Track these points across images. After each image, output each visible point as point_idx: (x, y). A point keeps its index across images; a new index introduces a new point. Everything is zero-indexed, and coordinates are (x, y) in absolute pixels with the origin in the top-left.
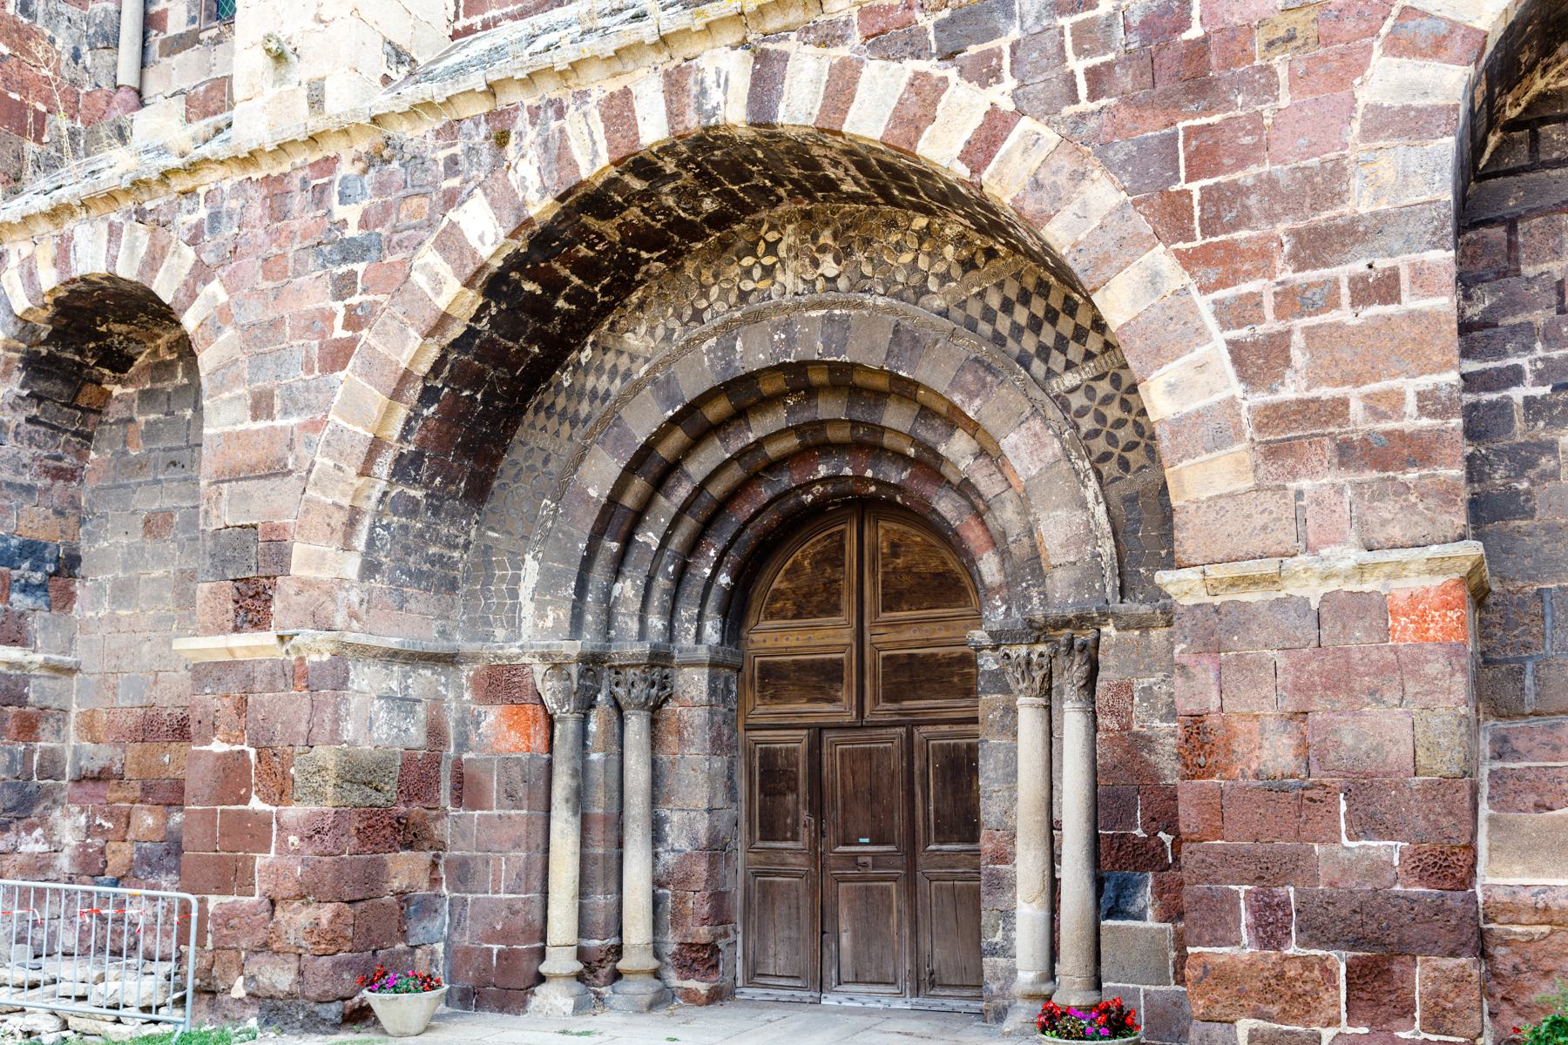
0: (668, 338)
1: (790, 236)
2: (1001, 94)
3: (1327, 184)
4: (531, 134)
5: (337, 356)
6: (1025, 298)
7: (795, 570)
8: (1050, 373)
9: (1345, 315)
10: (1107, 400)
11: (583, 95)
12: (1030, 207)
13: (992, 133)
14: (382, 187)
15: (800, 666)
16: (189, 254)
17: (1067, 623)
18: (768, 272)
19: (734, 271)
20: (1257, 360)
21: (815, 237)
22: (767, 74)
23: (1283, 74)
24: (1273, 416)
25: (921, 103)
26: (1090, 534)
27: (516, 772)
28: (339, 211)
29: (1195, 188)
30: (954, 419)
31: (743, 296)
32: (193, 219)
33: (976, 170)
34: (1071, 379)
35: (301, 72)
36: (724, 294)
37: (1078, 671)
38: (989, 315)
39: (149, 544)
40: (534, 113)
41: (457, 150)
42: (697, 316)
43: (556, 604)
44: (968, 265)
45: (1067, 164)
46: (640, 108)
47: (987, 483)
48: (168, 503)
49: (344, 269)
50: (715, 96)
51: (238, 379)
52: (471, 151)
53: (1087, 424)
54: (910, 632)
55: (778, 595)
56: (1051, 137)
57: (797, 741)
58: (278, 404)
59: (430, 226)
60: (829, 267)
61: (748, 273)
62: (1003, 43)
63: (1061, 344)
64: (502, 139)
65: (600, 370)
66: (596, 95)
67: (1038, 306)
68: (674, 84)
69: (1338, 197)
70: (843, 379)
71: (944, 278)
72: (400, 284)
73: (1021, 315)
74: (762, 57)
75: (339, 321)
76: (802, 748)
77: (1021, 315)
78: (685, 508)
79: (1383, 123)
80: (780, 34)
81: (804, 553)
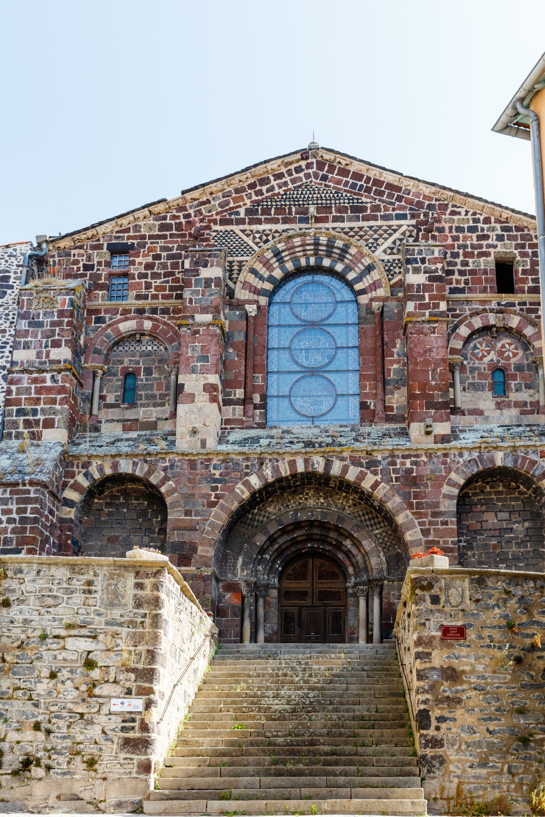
0: (280, 509)
1: (311, 493)
2: (379, 478)
3: (437, 505)
4: (269, 464)
5: (213, 505)
6: (367, 514)
7: (294, 569)
9: (439, 527)
11: (284, 459)
12: (384, 499)
13: (375, 485)
14: (226, 468)
15: (296, 592)
16: (163, 474)
17: (377, 580)
18: (306, 499)
19: (297, 498)
20: (425, 532)
22: (328, 464)
24: (427, 542)
25: (362, 477)
26: (381, 563)
27: (236, 609)
28: (213, 471)
30: (350, 536)
31: (300, 503)
32: (164, 465)
33: (373, 490)
34: (377, 531)
35: (199, 436)
36: (294, 502)
37: (378, 590)
38: (359, 516)
39: (109, 544)
40: (270, 460)
41: (249, 464)
42: (288, 506)
43: (247, 569)
44: (355, 505)
46: (298, 464)
47: (354, 551)
48: (117, 534)
50: (316, 466)
51: (180, 506)
52: (252, 465)
53: (381, 541)
54: (327, 585)
55: (289, 574)
56: (388, 487)
57: (296, 610)
58: (193, 514)
60: (322, 500)
61: (301, 498)
62: (379, 469)
63: (375, 524)
64: (262, 464)
65: (260, 515)
66: (287, 460)
67: (370, 516)
68: (306, 461)
69: (439, 507)
70: (322, 525)
72: (232, 490)
73: (367, 517)
74: (327, 460)
75: (213, 497)
76: (296, 612)
77: (367, 517)
78: (276, 550)
79: (446, 496)
80: (331, 457)
81: (297, 565)
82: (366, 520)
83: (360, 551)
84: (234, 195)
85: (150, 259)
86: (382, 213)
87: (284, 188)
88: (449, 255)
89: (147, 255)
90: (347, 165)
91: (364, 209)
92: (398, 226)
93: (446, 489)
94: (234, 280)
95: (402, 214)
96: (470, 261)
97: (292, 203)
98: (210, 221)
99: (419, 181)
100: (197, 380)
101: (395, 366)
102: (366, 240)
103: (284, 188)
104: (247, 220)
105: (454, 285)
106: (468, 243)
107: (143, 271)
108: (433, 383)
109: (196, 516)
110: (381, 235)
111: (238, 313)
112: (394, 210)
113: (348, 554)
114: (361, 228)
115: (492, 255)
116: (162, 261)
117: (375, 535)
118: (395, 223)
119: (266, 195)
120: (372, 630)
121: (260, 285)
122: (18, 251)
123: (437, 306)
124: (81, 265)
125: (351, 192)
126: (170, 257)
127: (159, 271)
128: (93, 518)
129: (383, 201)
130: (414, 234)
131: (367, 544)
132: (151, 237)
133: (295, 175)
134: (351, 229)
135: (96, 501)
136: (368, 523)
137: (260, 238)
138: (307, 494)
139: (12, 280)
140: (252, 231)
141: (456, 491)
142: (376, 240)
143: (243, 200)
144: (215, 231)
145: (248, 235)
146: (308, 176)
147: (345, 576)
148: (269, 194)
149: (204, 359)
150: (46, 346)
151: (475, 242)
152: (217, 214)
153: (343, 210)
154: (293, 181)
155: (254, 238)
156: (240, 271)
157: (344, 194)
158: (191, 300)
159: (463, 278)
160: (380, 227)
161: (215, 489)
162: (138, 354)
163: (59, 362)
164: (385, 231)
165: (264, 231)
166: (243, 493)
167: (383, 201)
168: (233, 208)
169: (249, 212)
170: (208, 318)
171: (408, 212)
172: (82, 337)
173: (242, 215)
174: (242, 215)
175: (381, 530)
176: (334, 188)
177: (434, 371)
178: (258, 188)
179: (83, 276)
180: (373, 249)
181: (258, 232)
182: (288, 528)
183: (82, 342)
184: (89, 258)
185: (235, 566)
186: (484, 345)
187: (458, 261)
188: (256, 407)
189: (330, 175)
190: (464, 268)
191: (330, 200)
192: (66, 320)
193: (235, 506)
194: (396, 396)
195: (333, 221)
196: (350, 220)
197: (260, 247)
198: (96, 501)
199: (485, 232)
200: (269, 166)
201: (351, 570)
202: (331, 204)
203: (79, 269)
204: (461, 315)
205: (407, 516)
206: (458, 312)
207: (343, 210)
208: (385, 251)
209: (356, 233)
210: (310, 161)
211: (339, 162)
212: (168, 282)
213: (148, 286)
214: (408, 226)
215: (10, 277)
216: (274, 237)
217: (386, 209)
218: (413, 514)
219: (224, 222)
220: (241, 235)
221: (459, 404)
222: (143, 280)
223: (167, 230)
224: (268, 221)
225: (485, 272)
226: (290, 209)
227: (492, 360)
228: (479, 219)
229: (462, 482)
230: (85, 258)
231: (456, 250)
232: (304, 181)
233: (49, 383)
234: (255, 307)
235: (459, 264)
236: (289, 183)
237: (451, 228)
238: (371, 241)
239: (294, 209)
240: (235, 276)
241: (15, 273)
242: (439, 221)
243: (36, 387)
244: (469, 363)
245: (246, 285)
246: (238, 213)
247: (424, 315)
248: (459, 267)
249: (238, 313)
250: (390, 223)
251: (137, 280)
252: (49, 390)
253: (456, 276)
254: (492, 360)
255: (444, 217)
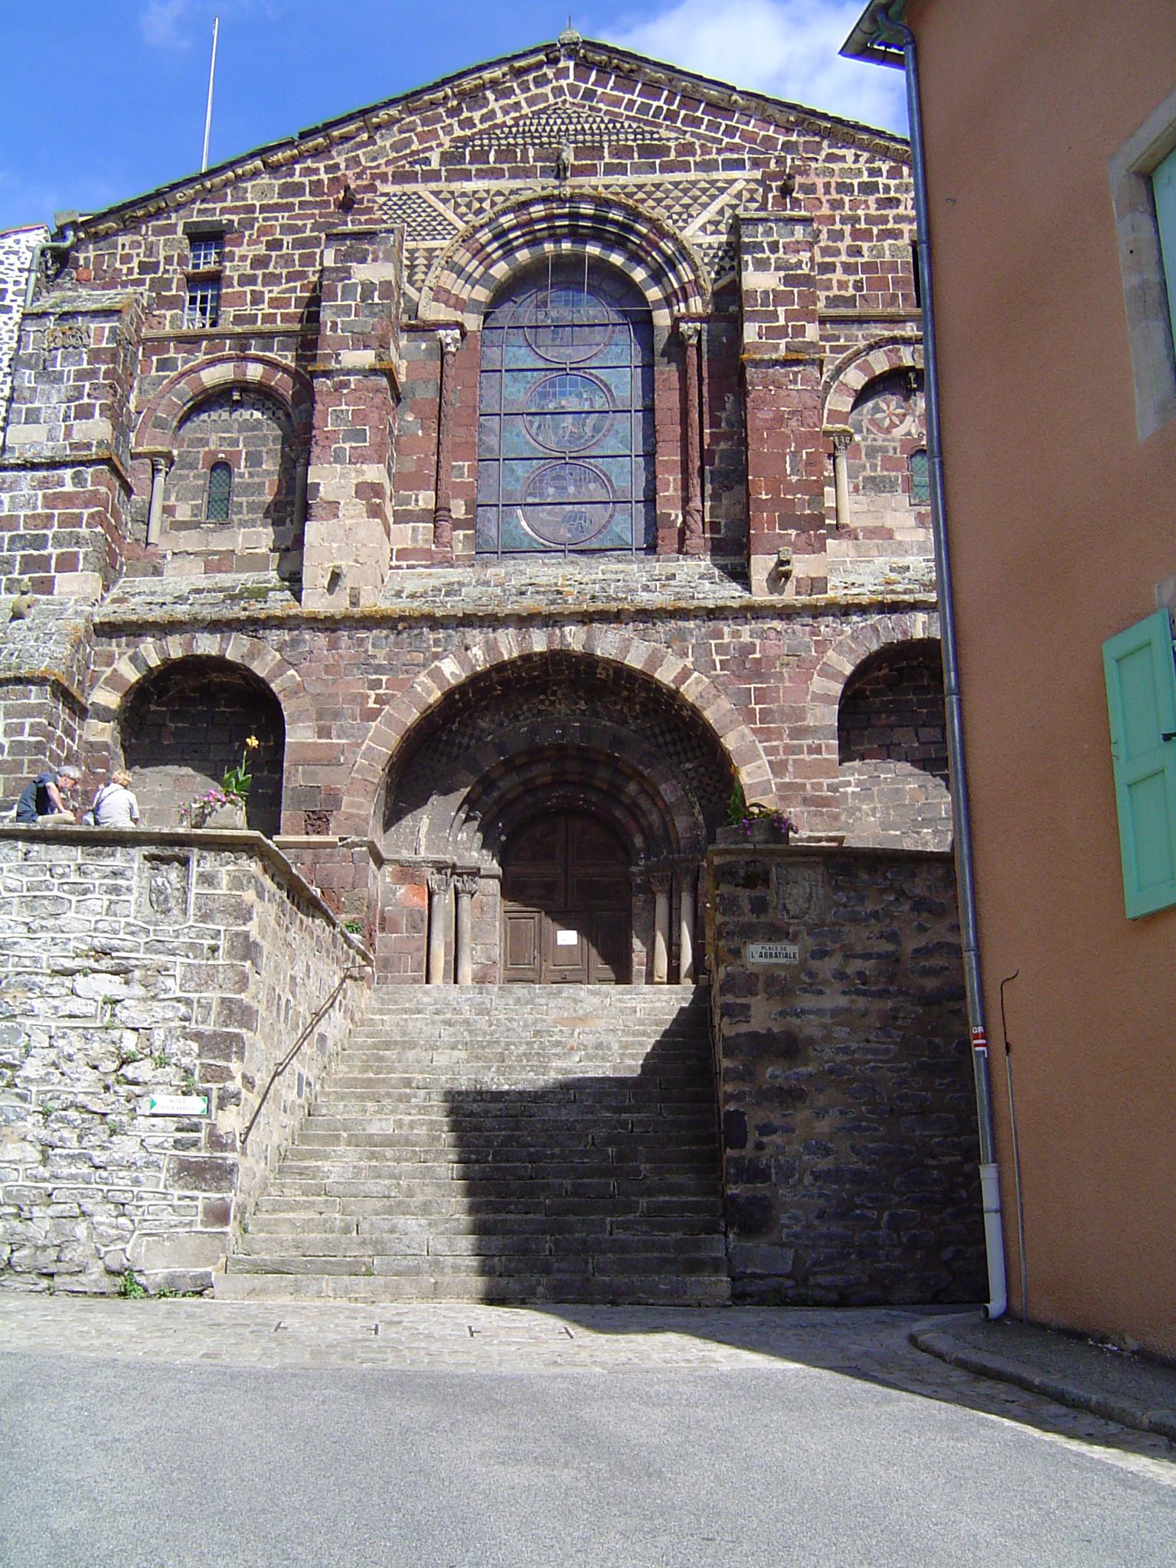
3: (800, 715)
5: (372, 715)
8: (680, 762)
9: (807, 758)
10: (703, 775)
12: (697, 704)
13: (685, 674)
18: (553, 703)
20: (778, 768)
21: (576, 692)
23: (786, 675)
29: (757, 707)
31: (540, 712)
34: (688, 766)
36: (529, 709)
38: (654, 735)
42: (516, 717)
44: (646, 714)
45: (714, 692)
47: (644, 803)
49: (374, 677)
53: (695, 784)
59: (424, 666)
61: (542, 702)
63: (685, 752)
65: (463, 736)
69: (804, 719)
71: (635, 718)
72: (407, 687)
73: (668, 738)
77: (668, 738)
79: (816, 697)
82: (666, 744)
83: (656, 805)
84: (419, 129)
85: (261, 249)
86: (698, 159)
87: (514, 114)
88: (824, 236)
89: (257, 242)
90: (631, 71)
91: (665, 151)
92: (726, 181)
93: (817, 684)
94: (419, 284)
95: (736, 160)
96: (865, 246)
97: (529, 140)
98: (374, 177)
99: (767, 100)
100: (343, 476)
101: (723, 446)
102: (668, 208)
103: (514, 114)
104: (443, 174)
105: (835, 292)
106: (860, 212)
107: (249, 272)
108: (794, 479)
109: (339, 737)
110: (695, 199)
111: (424, 346)
112: (719, 151)
113: (633, 810)
114: (657, 186)
115: (906, 235)
116: (285, 251)
117: (685, 772)
118: (721, 175)
119: (479, 127)
120: (679, 959)
121: (465, 292)
122: (23, 244)
123: (800, 331)
124: (135, 264)
125: (639, 120)
126: (298, 244)
127: (278, 271)
128: (147, 741)
129: (699, 136)
130: (758, 196)
131: (669, 792)
132: (264, 209)
133: (534, 91)
134: (640, 187)
135: (153, 708)
136: (672, 749)
137: (469, 206)
138: (554, 693)
139: (9, 296)
140: (452, 193)
141: (837, 688)
142: (687, 206)
143: (437, 137)
144: (382, 195)
145: (445, 201)
146: (558, 92)
147: (629, 855)
148: (486, 125)
149: (357, 435)
150: (66, 418)
151: (873, 212)
152: (387, 164)
153: (627, 152)
154: (531, 102)
155: (457, 205)
156: (428, 267)
157: (626, 125)
158: (334, 324)
159: (852, 278)
160: (694, 183)
161: (376, 685)
162: (236, 426)
163: (88, 446)
164: (704, 191)
165: (475, 192)
166: (429, 693)
167: (699, 136)
168: (418, 152)
169: (445, 158)
170: (366, 358)
171: (746, 156)
172: (132, 397)
173: (435, 164)
174: (435, 164)
175: (696, 763)
176: (607, 112)
177: (794, 454)
178: (466, 114)
179: (139, 283)
180: (680, 224)
181: (464, 194)
182: (519, 761)
183: (132, 407)
184: (151, 250)
185: (415, 831)
186: (893, 405)
187: (842, 246)
188: (458, 525)
189: (600, 90)
190: (852, 260)
191: (601, 135)
192: (104, 367)
193: (413, 716)
194: (724, 502)
195: (606, 173)
196: (638, 170)
197: (467, 222)
198: (153, 708)
199: (892, 194)
200: (487, 75)
201: (638, 841)
202: (601, 142)
203: (130, 271)
204: (847, 348)
205: (743, 736)
206: (842, 342)
207: (627, 152)
208: (703, 228)
209: (649, 194)
210: (561, 65)
211: (617, 67)
212: (293, 290)
213: (257, 298)
214: (748, 181)
215: (6, 290)
216: (493, 204)
217: (705, 150)
218: (754, 731)
219: (401, 177)
220: (432, 199)
221: (846, 518)
222: (248, 289)
223: (294, 195)
224: (482, 175)
225: (893, 267)
226: (525, 152)
227: (909, 433)
228: (880, 169)
229: (848, 669)
230: (142, 251)
231: (838, 226)
232: (552, 100)
233: (69, 487)
234: (457, 333)
235: (843, 250)
236: (523, 104)
237: (827, 186)
238: (678, 208)
239: (531, 152)
240: (419, 276)
241: (16, 283)
242: (805, 173)
243: (45, 496)
244: (865, 439)
245: (440, 294)
246: (427, 161)
247: (776, 348)
248: (844, 258)
249: (424, 346)
250: (715, 175)
251: (237, 289)
252: (68, 499)
253: (838, 275)
254: (909, 433)
255: (813, 165)
